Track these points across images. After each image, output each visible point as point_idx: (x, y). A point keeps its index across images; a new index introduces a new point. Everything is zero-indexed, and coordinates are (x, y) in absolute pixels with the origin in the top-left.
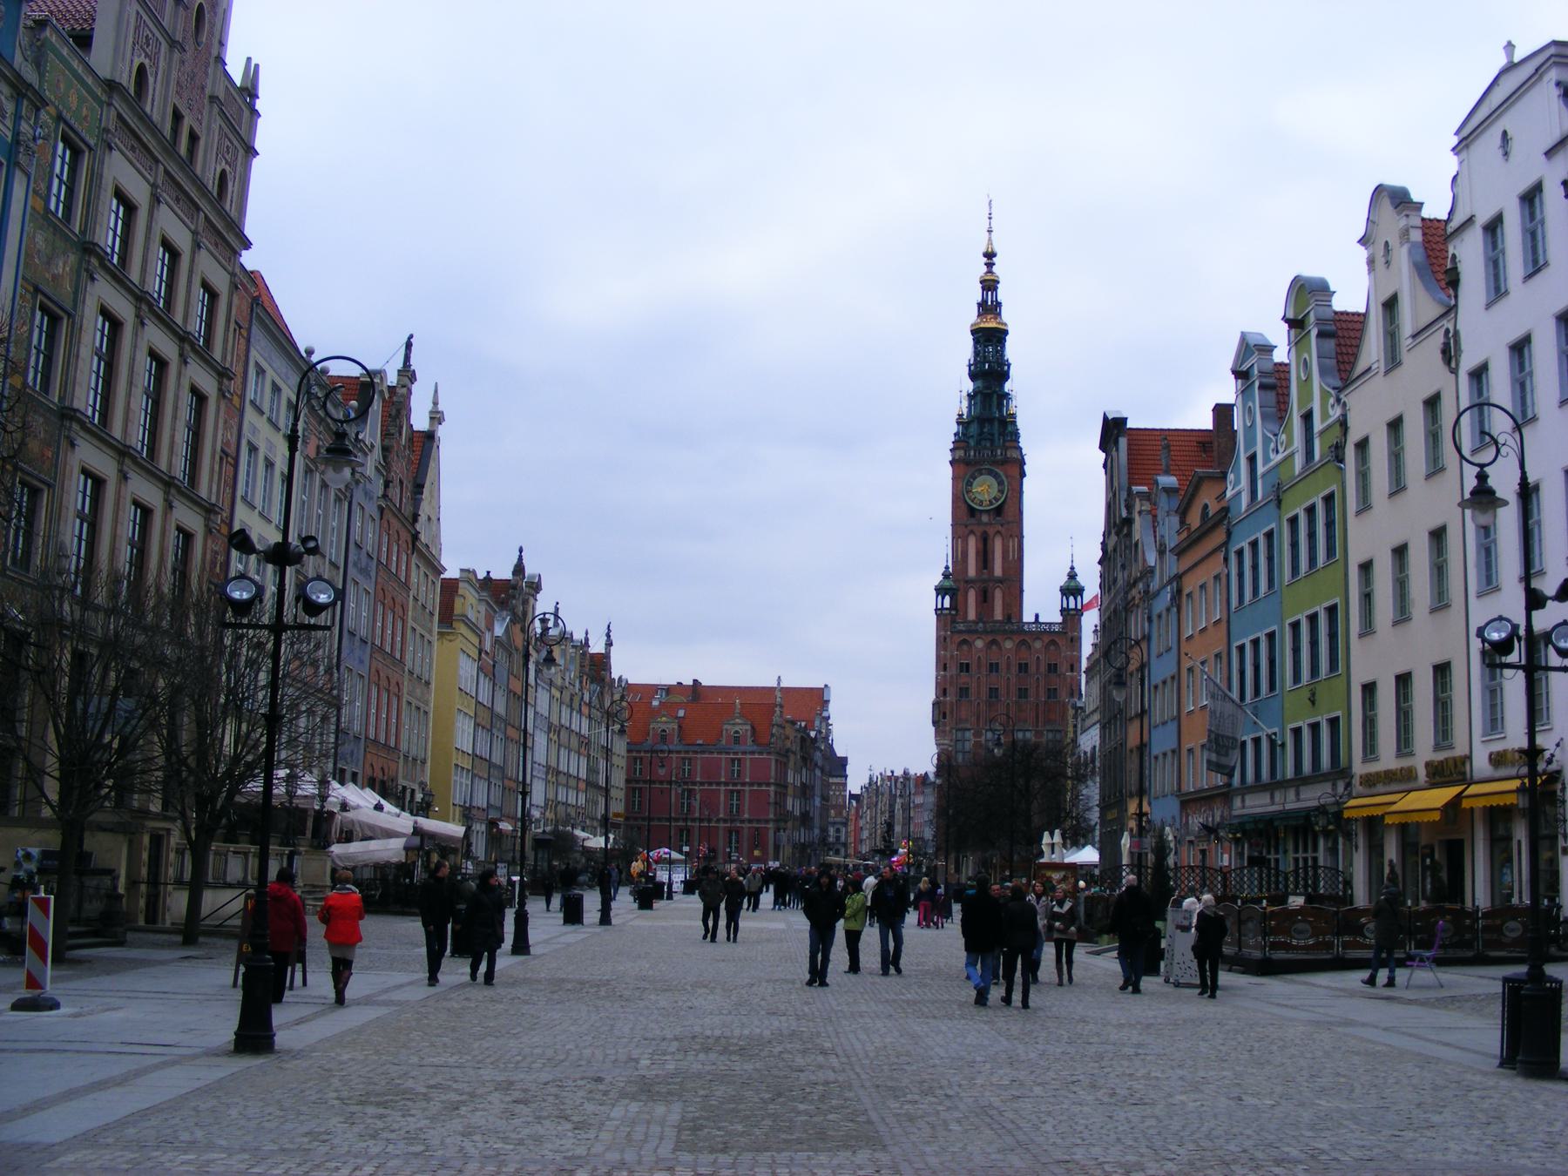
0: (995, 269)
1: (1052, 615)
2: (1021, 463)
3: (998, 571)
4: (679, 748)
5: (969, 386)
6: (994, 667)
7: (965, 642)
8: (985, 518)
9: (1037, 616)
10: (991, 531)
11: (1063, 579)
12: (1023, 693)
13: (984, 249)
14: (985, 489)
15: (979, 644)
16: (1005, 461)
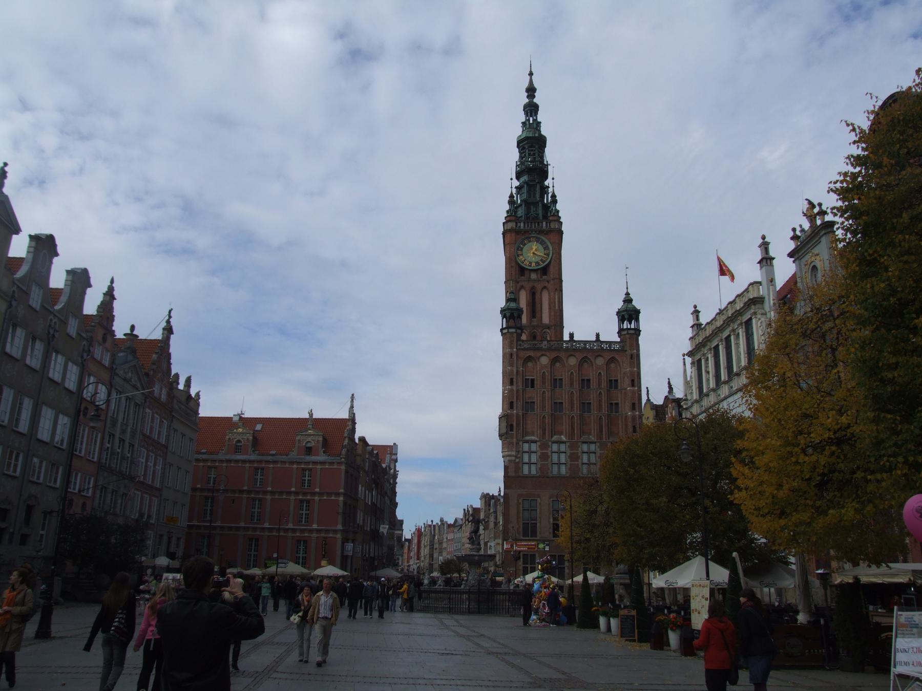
0: (535, 100)
1: (610, 334)
2: (562, 233)
3: (546, 320)
4: (253, 457)
5: (516, 183)
6: (556, 383)
7: (529, 359)
8: (534, 276)
9: (598, 335)
10: (539, 287)
11: (620, 304)
12: (585, 406)
13: (526, 84)
14: (533, 253)
15: (544, 360)
16: (548, 232)
